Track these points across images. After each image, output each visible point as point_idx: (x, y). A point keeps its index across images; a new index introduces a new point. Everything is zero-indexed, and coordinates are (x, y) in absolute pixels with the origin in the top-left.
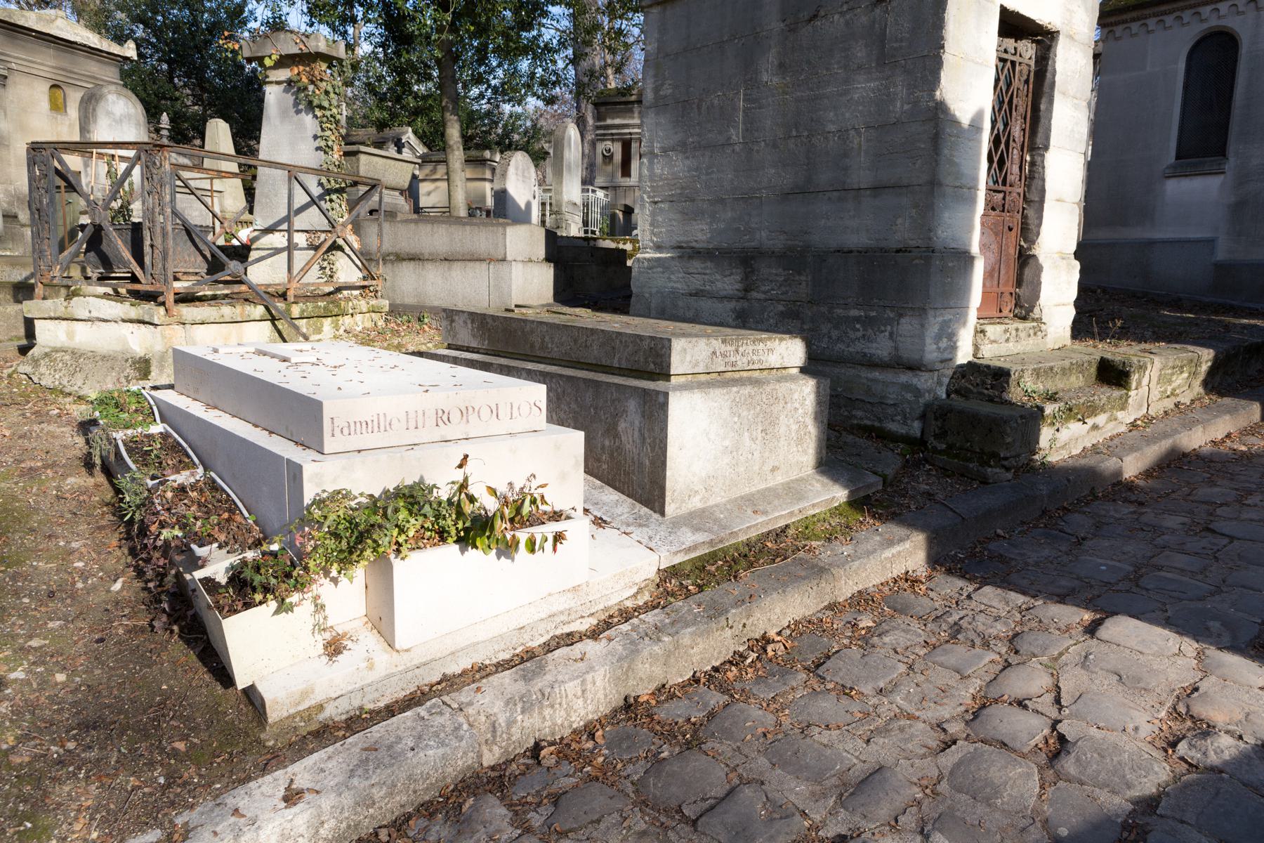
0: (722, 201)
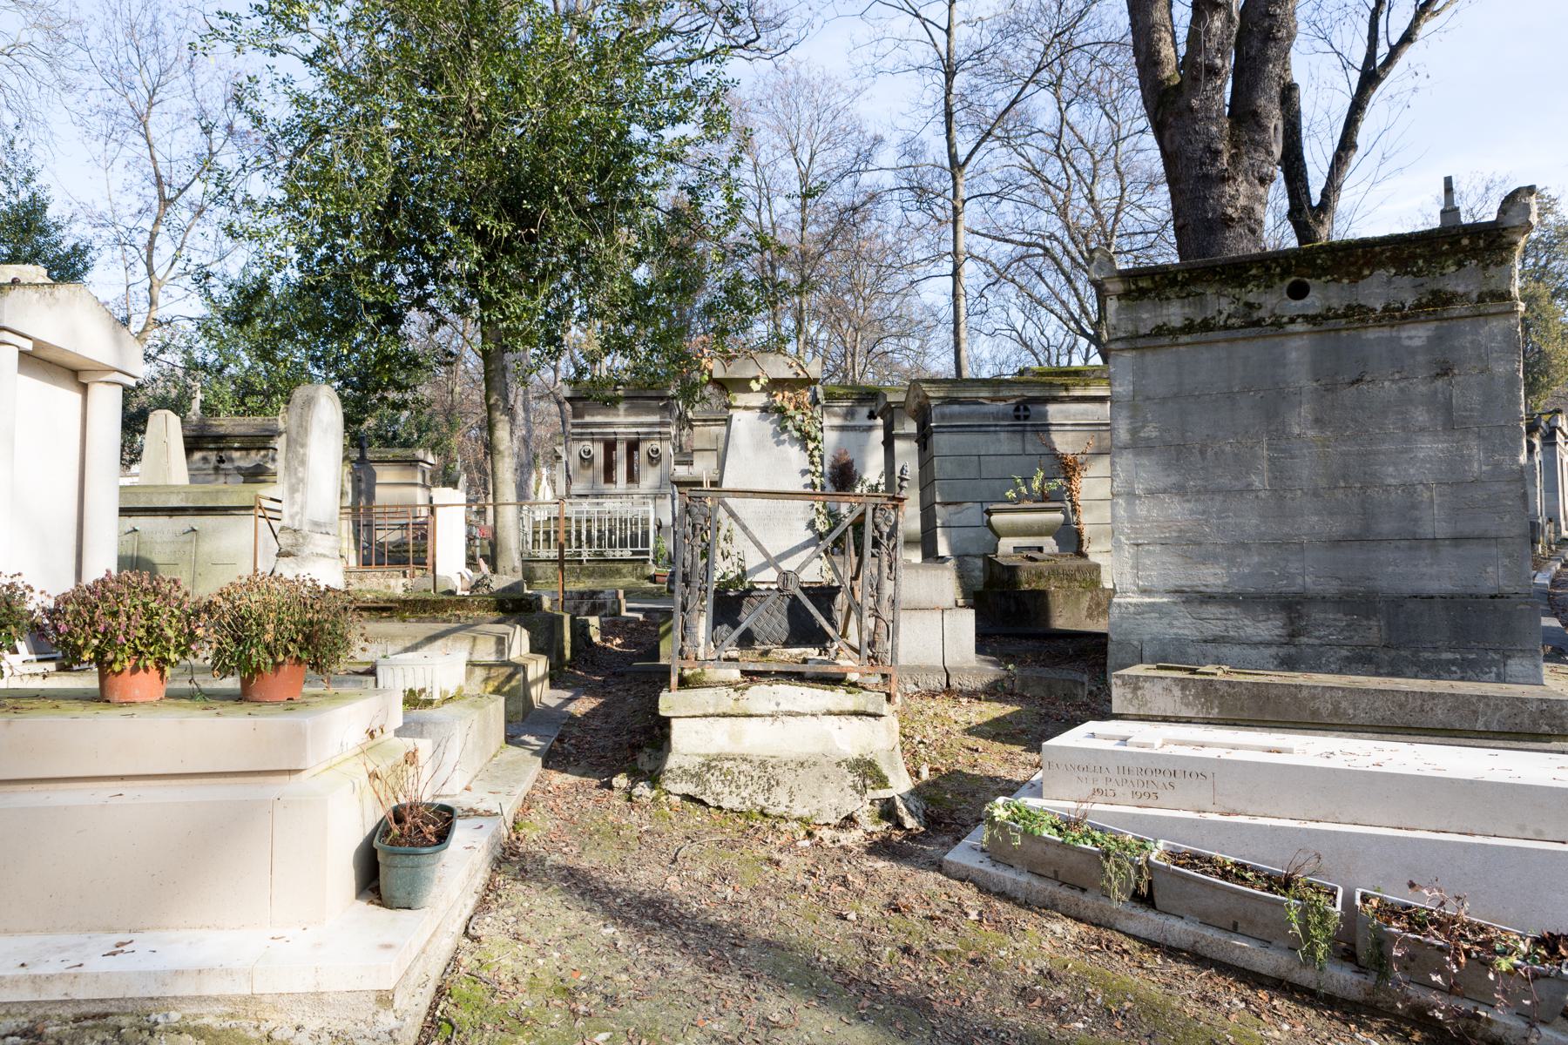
0: (1244, 545)
